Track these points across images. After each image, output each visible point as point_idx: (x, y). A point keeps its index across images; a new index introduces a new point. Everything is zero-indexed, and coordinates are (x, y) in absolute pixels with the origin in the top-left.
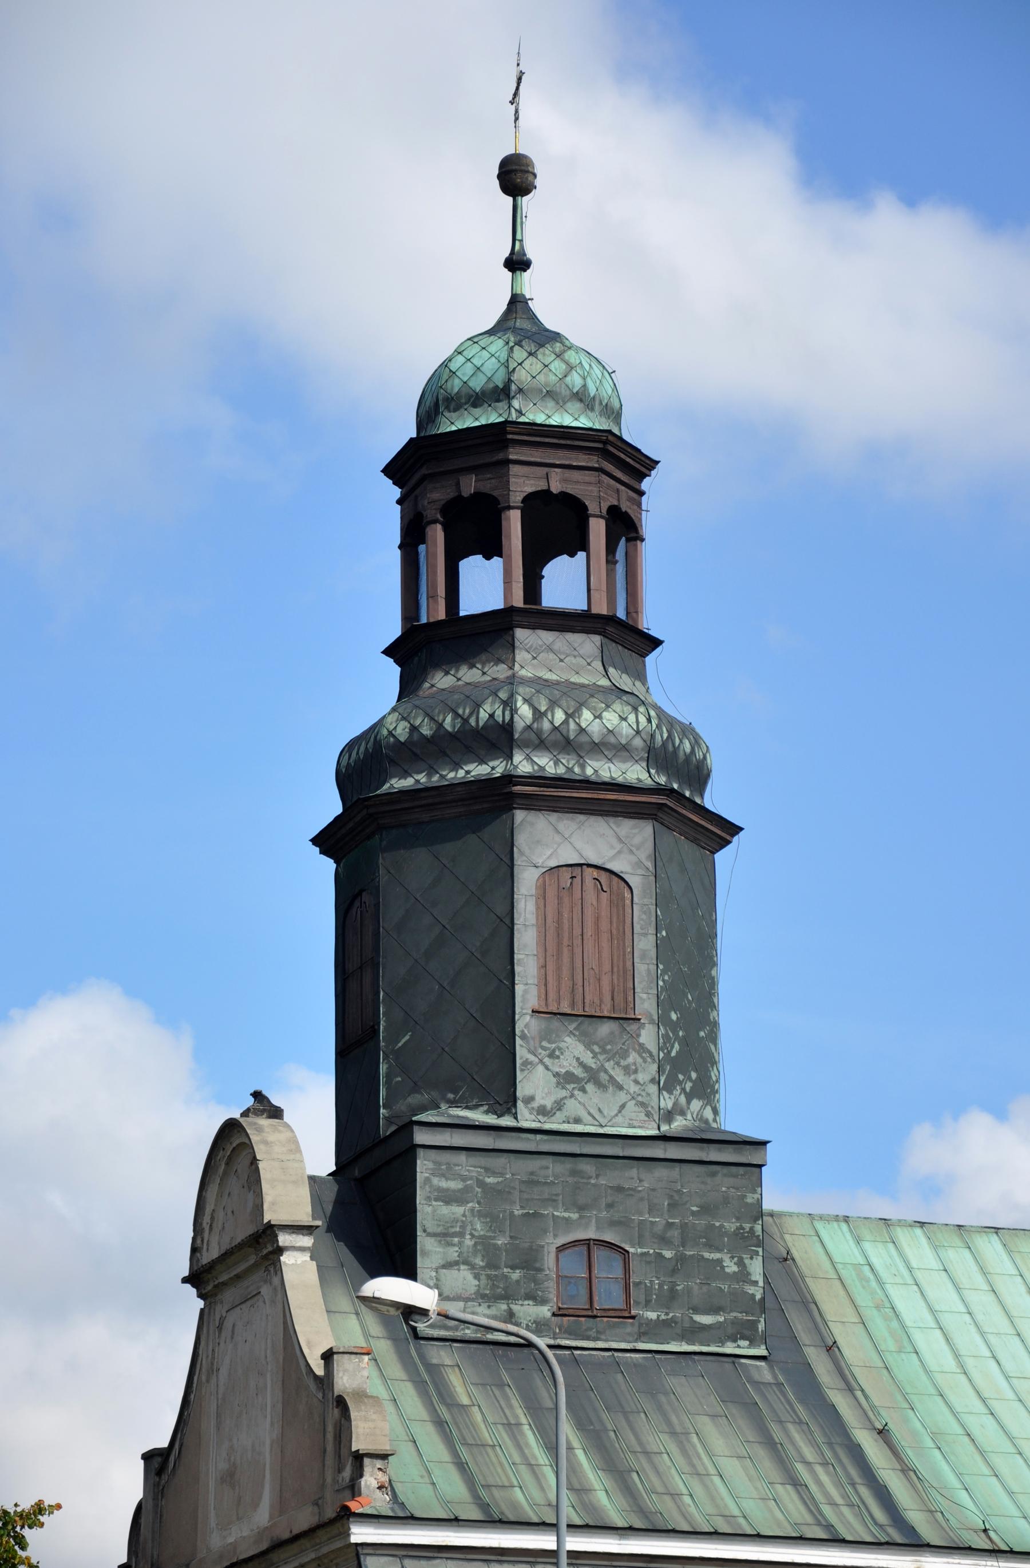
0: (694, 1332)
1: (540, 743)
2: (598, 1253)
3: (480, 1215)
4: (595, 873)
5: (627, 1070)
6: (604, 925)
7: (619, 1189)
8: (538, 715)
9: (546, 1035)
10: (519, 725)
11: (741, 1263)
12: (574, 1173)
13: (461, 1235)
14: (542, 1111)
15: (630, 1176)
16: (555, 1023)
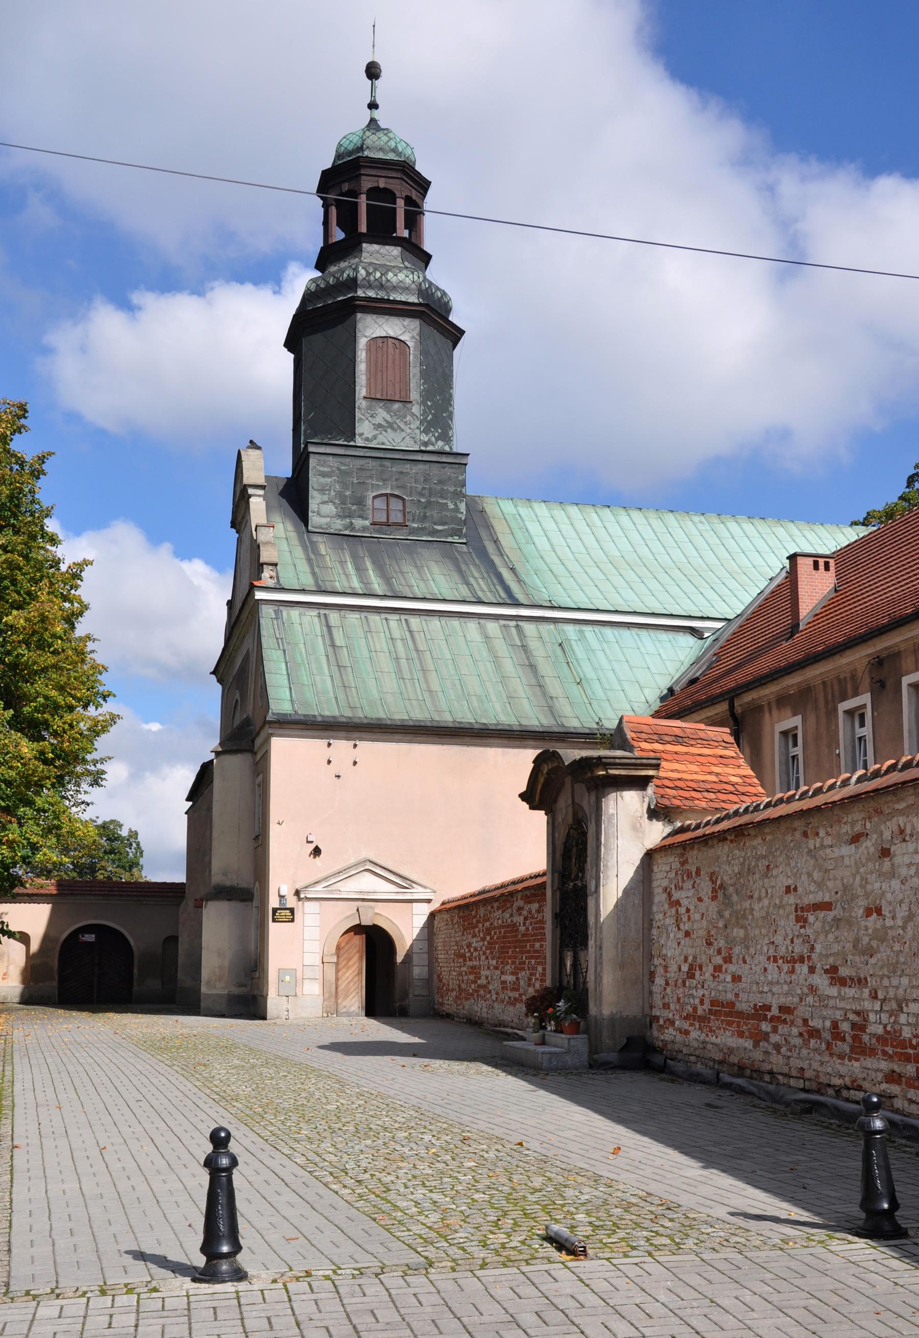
0: (434, 532)
1: (370, 286)
2: (392, 500)
3: (338, 482)
4: (393, 341)
5: (406, 423)
6: (397, 362)
7: (402, 473)
8: (368, 274)
9: (369, 408)
10: (360, 278)
11: (456, 504)
12: (381, 466)
13: (330, 490)
14: (367, 439)
15: (407, 467)
16: (374, 403)
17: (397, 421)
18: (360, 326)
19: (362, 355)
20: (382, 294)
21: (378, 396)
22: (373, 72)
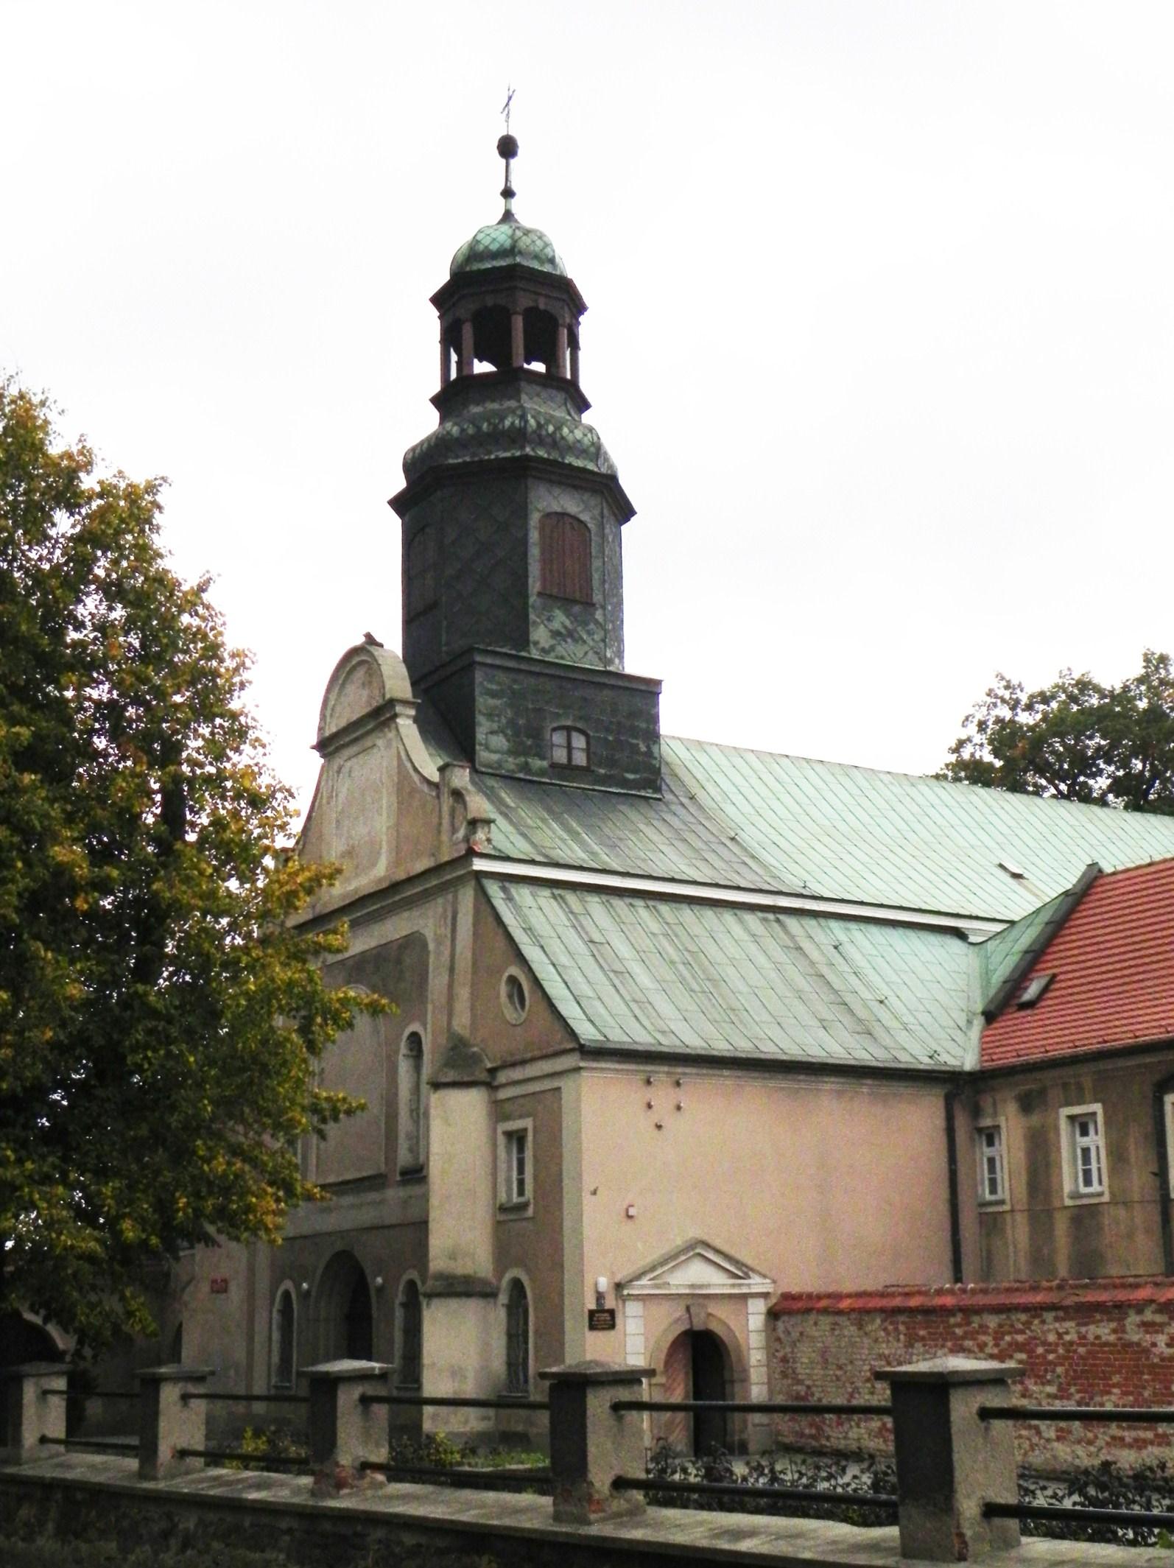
1: (541, 442)
2: (574, 734)
5: (589, 633)
7: (585, 699)
10: (529, 430)
12: (561, 688)
13: (498, 716)
17: (579, 629)
18: (532, 495)
19: (534, 536)
20: (554, 455)
21: (555, 592)
22: (507, 148)
